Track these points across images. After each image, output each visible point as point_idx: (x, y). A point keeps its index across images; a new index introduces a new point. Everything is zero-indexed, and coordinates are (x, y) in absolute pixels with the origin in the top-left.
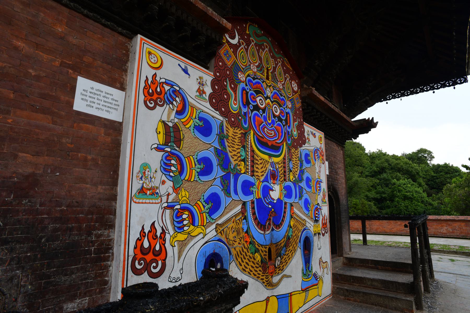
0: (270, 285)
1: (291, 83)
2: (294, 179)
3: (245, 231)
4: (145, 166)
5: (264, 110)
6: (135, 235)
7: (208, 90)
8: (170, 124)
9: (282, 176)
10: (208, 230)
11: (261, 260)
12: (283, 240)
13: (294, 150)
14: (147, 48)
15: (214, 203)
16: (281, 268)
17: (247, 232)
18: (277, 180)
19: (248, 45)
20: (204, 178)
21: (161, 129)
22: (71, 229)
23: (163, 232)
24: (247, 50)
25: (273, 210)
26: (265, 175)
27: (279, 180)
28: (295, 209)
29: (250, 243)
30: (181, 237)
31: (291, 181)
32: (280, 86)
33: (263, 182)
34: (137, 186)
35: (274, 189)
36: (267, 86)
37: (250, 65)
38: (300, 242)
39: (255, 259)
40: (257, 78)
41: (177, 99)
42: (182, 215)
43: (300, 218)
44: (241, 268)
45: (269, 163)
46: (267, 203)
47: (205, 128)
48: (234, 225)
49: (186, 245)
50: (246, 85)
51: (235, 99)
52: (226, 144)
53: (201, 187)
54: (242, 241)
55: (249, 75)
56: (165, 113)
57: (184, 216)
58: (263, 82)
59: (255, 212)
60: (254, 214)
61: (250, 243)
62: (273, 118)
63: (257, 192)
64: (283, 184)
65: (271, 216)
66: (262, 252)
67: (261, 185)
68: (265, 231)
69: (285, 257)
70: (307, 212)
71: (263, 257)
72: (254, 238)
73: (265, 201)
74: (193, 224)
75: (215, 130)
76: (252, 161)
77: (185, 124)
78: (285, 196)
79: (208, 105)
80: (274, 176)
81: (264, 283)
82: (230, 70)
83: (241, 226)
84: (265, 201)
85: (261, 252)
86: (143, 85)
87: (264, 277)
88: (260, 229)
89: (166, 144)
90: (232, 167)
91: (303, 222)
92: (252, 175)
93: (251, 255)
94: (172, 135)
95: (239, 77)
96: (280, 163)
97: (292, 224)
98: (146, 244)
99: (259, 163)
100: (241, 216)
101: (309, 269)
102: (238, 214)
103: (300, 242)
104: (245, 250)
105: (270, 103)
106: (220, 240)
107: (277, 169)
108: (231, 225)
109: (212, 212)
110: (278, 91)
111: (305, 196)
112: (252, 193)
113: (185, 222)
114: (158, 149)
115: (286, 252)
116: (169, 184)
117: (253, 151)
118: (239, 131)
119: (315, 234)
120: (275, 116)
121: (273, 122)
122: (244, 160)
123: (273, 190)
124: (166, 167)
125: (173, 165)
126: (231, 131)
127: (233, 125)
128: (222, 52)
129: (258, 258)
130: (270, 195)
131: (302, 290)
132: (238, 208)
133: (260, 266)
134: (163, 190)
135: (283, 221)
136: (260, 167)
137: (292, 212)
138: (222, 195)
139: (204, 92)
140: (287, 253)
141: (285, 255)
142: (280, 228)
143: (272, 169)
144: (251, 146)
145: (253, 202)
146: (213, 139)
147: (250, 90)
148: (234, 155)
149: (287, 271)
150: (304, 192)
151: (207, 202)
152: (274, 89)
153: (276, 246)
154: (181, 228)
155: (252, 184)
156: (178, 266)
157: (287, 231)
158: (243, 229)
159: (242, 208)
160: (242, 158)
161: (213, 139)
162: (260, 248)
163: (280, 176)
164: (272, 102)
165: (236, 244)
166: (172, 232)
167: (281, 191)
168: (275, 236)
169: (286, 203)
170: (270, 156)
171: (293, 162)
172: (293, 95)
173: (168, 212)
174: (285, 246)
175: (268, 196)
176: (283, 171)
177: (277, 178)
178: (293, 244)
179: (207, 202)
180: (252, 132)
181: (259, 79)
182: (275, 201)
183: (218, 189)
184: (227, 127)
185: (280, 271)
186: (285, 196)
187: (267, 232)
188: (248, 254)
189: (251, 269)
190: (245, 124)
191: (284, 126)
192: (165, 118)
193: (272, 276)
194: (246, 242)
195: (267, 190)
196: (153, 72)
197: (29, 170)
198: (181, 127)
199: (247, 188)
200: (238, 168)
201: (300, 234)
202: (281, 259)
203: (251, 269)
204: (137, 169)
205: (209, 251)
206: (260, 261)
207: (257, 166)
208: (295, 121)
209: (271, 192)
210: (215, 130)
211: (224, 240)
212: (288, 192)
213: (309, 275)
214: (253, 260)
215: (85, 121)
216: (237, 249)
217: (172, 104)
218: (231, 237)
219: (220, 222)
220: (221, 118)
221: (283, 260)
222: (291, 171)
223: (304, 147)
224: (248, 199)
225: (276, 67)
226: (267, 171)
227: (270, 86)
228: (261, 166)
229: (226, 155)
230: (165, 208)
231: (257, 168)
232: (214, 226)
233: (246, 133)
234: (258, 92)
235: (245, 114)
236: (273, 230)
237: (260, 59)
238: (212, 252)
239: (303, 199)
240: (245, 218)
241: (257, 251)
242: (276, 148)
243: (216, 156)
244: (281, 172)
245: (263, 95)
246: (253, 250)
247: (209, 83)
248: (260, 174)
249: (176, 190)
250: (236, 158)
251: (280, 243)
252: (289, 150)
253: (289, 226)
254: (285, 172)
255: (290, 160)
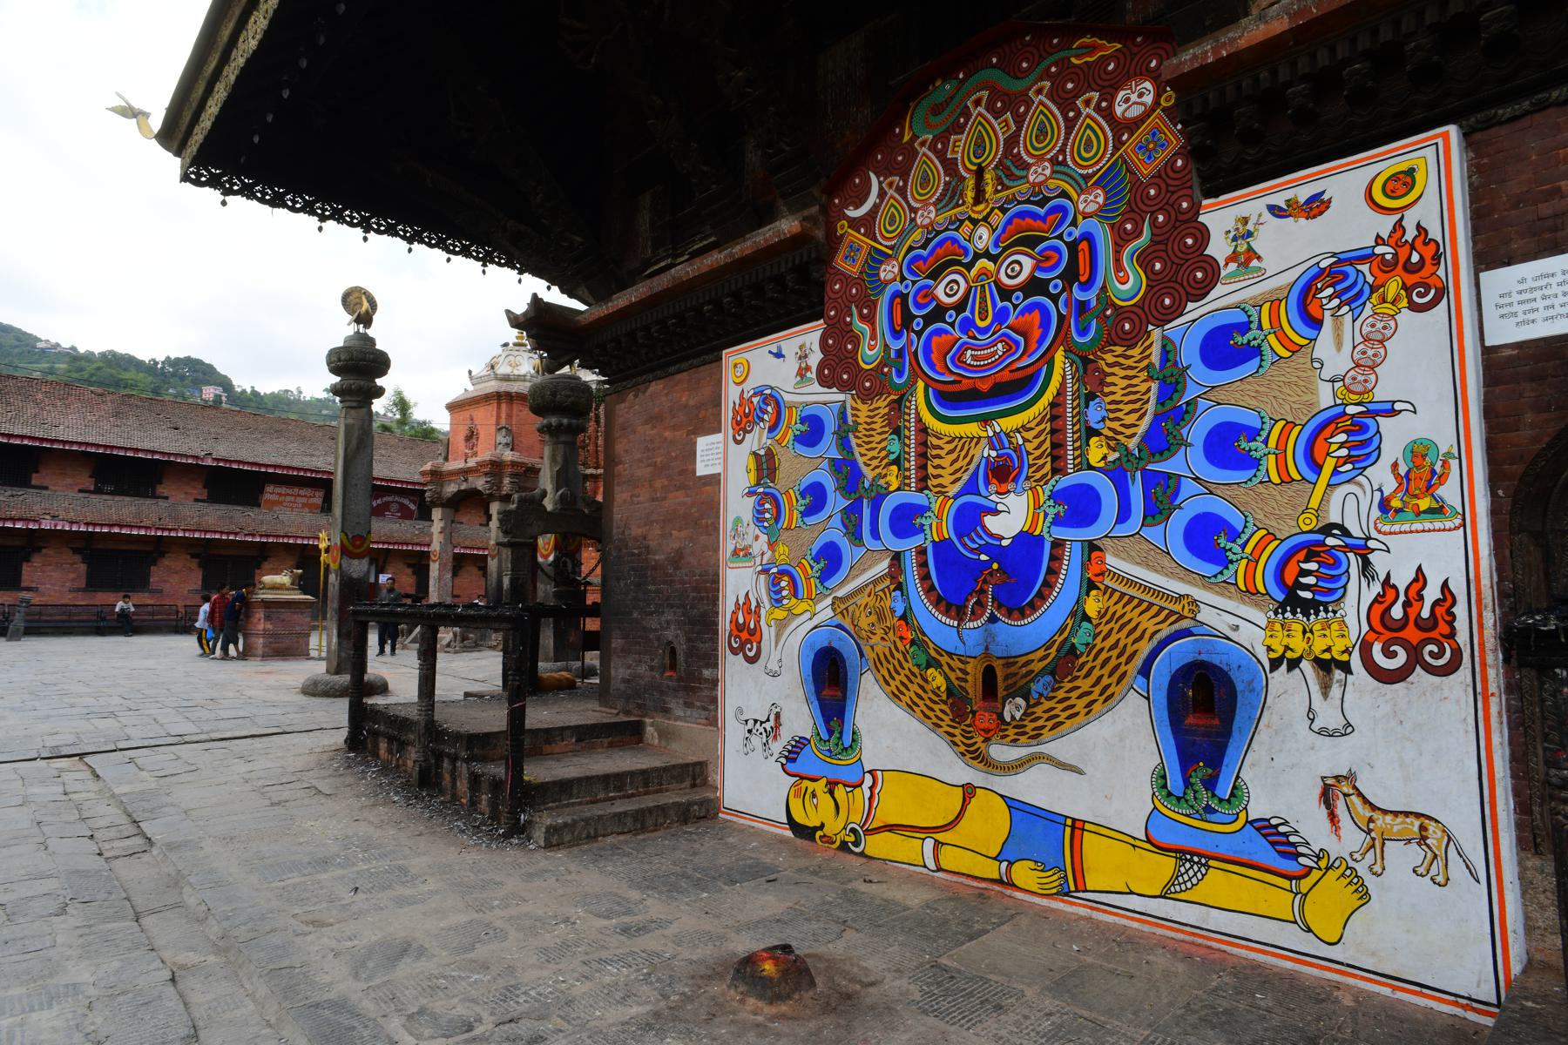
0: (976, 756)
1: (1108, 114)
2: (1113, 456)
3: (899, 613)
4: (738, 520)
5: (960, 307)
6: (730, 607)
7: (815, 358)
8: (762, 452)
9: (1041, 462)
10: (819, 607)
11: (949, 692)
12: (1041, 653)
13: (1119, 350)
14: (732, 360)
15: (830, 559)
16: (1027, 729)
17: (904, 617)
18: (1015, 480)
19: (905, 176)
20: (811, 520)
21: (752, 465)
22: (702, 599)
23: (758, 606)
24: (902, 191)
25: (995, 566)
26: (966, 477)
27: (1028, 478)
28: (1111, 560)
29: (913, 643)
30: (780, 614)
31: (1090, 467)
32: (1039, 173)
33: (955, 497)
34: (730, 548)
35: (1000, 507)
36: (975, 222)
37: (913, 220)
38: (1145, 671)
39: (926, 681)
40: (938, 233)
41: (769, 409)
42: (781, 580)
43: (1147, 589)
44: (888, 689)
45: (984, 442)
46: (972, 550)
47: (812, 432)
48: (871, 601)
49: (785, 626)
50: (903, 279)
51: (873, 337)
52: (854, 441)
53: (806, 536)
54: (891, 634)
55: (911, 249)
56: (757, 439)
57: (783, 584)
58: (957, 230)
59: (928, 574)
60: (925, 577)
61: (913, 643)
62: (1000, 304)
63: (938, 525)
64: (1049, 487)
65: (985, 582)
66: (952, 669)
67: (951, 507)
68: (961, 620)
69: (1047, 705)
70: (1209, 569)
71: (956, 683)
72: (924, 634)
73: (965, 546)
74: (796, 596)
75: (831, 425)
76: (923, 456)
77: (779, 442)
78: (1057, 521)
79: (816, 387)
80: (1002, 473)
81: (956, 744)
82: (858, 282)
83: (888, 603)
84: (965, 546)
85: (946, 668)
86: (731, 414)
87: (957, 732)
88: (947, 613)
89: (758, 484)
90: (867, 484)
91: (1177, 608)
92: (920, 490)
93: (915, 670)
94: (766, 465)
95: (882, 275)
96: (1032, 425)
97: (1092, 607)
98: (741, 620)
99: (943, 453)
100: (888, 582)
101: (1210, 784)
102: (882, 579)
103: (1145, 671)
104: (900, 656)
105: (990, 266)
106: (839, 626)
107: (1017, 449)
108: (863, 599)
109: (825, 576)
110: (1028, 202)
111: (1192, 504)
112: (921, 529)
113: (785, 593)
114: (751, 493)
115: (1054, 690)
116: (764, 538)
117: (923, 430)
118: (882, 404)
119: (1275, 664)
120: (1005, 293)
121: (1001, 316)
122: (897, 462)
123: (995, 512)
124: (759, 518)
125: (767, 511)
126: (864, 408)
127: (866, 396)
128: (840, 263)
129: (937, 680)
130: (984, 527)
131: (1149, 841)
132: (883, 566)
133: (945, 702)
134: (756, 550)
135: (1042, 597)
136: (945, 462)
137: (1095, 569)
138: (844, 544)
139: (808, 368)
140: (1061, 694)
141: (1050, 699)
142: (1023, 616)
143: (994, 454)
144: (919, 420)
145: (921, 552)
146: (828, 447)
147: (914, 283)
148: (874, 458)
149: (1055, 747)
150: (1188, 487)
151: (816, 559)
152: (1004, 210)
153: (1008, 665)
154: (779, 601)
155: (921, 510)
156: (775, 656)
157: (1062, 630)
158: (893, 611)
159: (890, 567)
160: (892, 457)
161: (828, 447)
162: (944, 660)
163: (1030, 466)
164: (993, 259)
165: (875, 640)
166: (768, 606)
167: (1037, 506)
168: (1001, 638)
169: (1058, 544)
170: (985, 420)
171: (1108, 399)
172: (1118, 144)
173: (762, 577)
174: (1053, 673)
175: (974, 530)
176: (1047, 444)
177: (1019, 475)
178: (1096, 673)
179: (816, 559)
180: (921, 384)
181: (947, 229)
182: (1005, 543)
183: (837, 535)
184: (853, 409)
185: (1023, 739)
186: (1057, 521)
187: (971, 625)
188: (906, 665)
189: (916, 699)
190: (900, 374)
191: (1055, 298)
192: (755, 448)
193: (987, 740)
194: (901, 638)
195: (970, 518)
196: (739, 389)
197: (676, 545)
198: (776, 449)
199: (905, 520)
200: (882, 482)
201: (1145, 648)
202: (1029, 706)
203: (916, 699)
204: (730, 526)
205: (822, 643)
206: (943, 689)
207: (937, 462)
208: (1121, 239)
209: (989, 521)
210: (831, 425)
211: (850, 628)
212: (1080, 507)
213: (1209, 810)
214: (919, 680)
215: (705, 485)
216: (878, 649)
217: (762, 420)
218: (864, 622)
219: (840, 593)
220: (841, 397)
221: (1039, 710)
222: (1092, 432)
223: (1194, 310)
224: (908, 545)
225: (1019, 129)
226: (972, 467)
227: (985, 219)
228: (954, 456)
229: (854, 464)
230: (760, 572)
231: (939, 467)
232: (829, 601)
233: (902, 396)
234: (935, 275)
235: (900, 353)
236: (993, 619)
237: (950, 167)
238: (826, 644)
239: (1178, 521)
240: (899, 587)
241: (932, 663)
242: (1015, 388)
243: (832, 474)
244: (1038, 453)
245: (959, 263)
246: (922, 659)
247: (816, 347)
248: (946, 481)
249: (772, 545)
250: (875, 463)
251: (1024, 659)
252: (1085, 363)
253: (1073, 614)
254: (1057, 446)
255: (1091, 397)
